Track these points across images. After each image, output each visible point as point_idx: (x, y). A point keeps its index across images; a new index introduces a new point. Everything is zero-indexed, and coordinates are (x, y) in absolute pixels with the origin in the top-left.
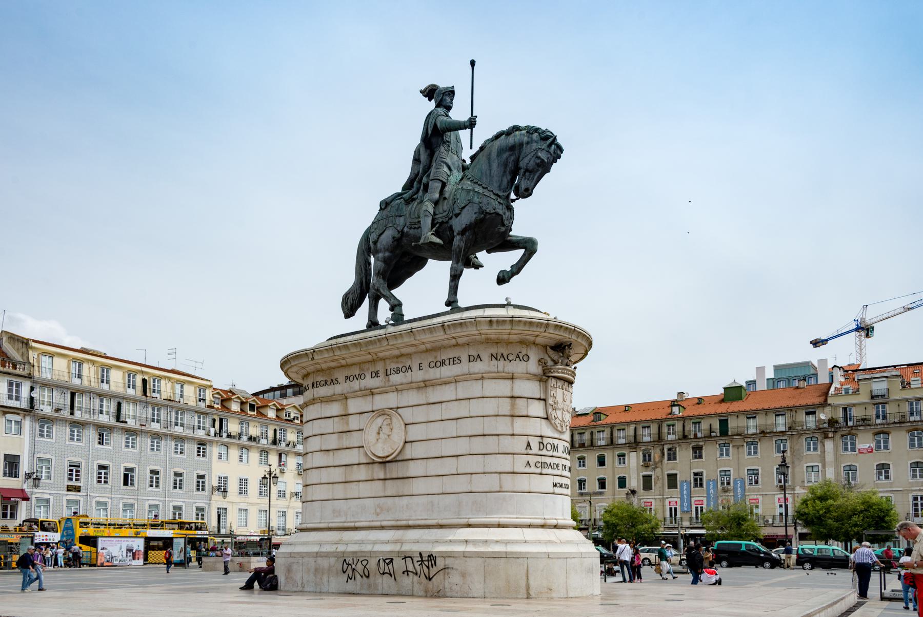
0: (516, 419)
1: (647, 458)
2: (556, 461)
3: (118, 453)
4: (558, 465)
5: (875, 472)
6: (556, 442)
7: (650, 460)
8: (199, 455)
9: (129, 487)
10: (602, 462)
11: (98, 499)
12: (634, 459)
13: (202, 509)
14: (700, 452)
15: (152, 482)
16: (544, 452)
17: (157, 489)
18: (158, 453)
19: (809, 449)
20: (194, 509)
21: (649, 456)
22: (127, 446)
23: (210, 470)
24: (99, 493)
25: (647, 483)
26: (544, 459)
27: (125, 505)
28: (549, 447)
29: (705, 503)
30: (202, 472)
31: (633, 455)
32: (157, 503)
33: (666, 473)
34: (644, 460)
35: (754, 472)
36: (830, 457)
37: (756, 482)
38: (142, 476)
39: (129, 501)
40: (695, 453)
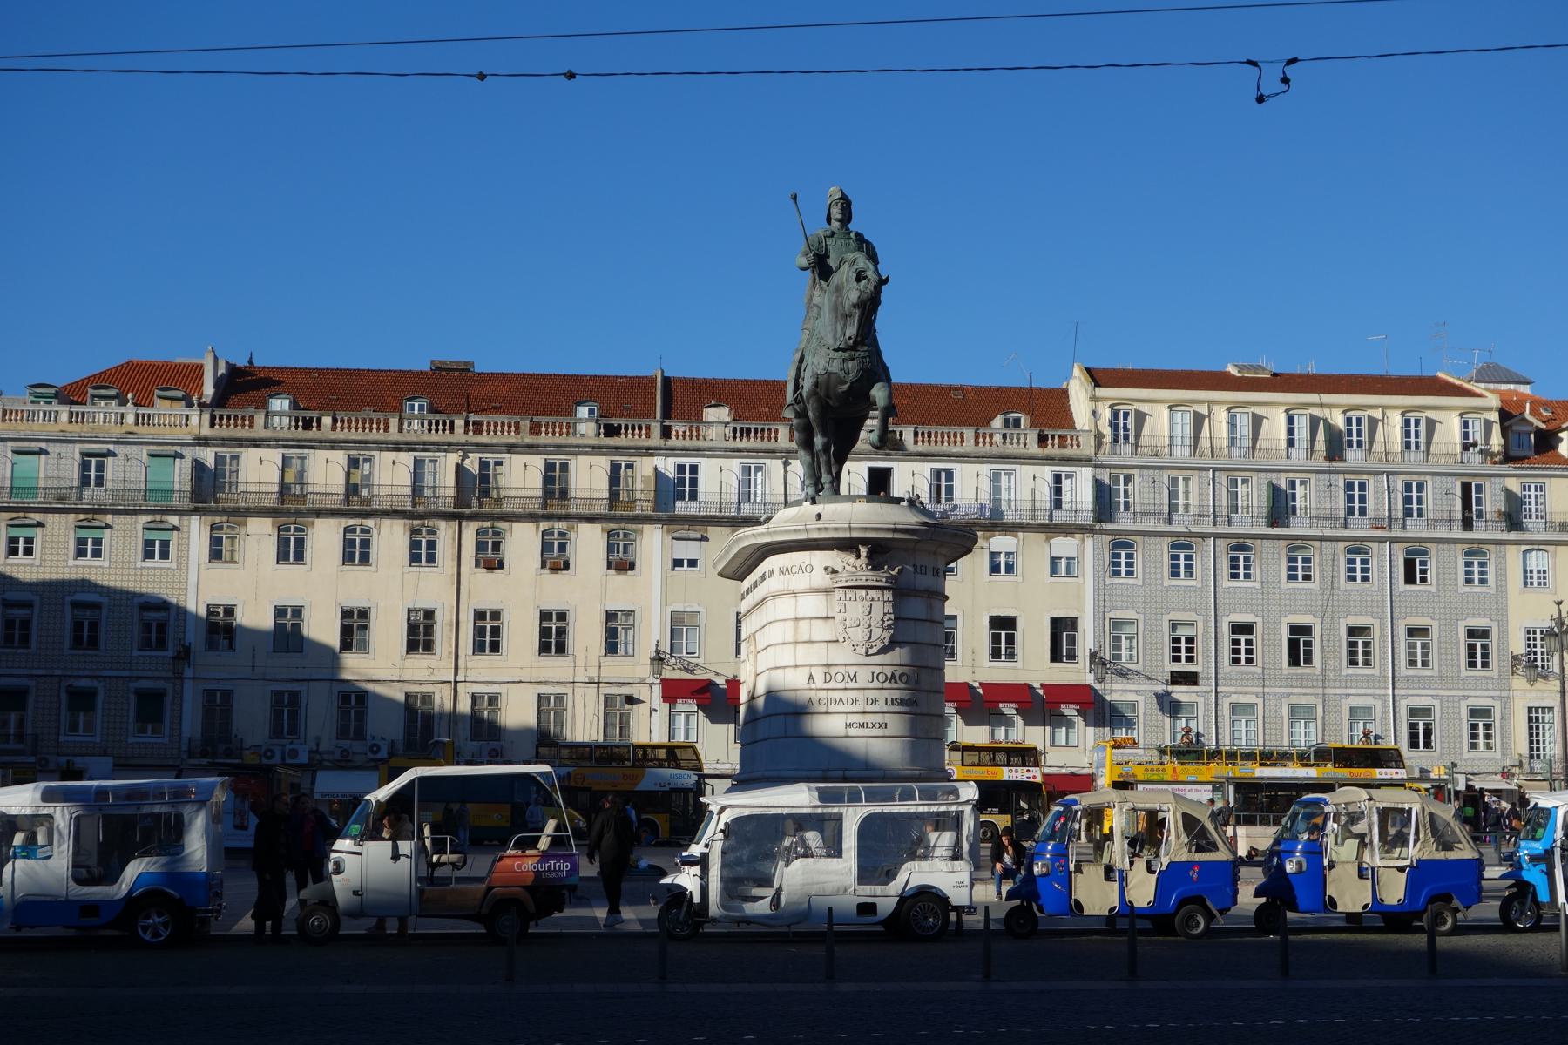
0: (799, 647)
2: (852, 694)
3: (1272, 598)
4: (855, 701)
6: (852, 671)
8: (1469, 582)
9: (1302, 670)
11: (1234, 698)
13: (1485, 713)
15: (1353, 653)
16: (832, 685)
17: (1367, 671)
18: (1366, 585)
20: (1464, 713)
22: (1293, 578)
23: (1502, 616)
24: (1240, 687)
26: (831, 694)
27: (1293, 710)
28: (839, 677)
30: (1479, 623)
32: (1369, 701)
38: (1330, 642)
39: (1304, 700)
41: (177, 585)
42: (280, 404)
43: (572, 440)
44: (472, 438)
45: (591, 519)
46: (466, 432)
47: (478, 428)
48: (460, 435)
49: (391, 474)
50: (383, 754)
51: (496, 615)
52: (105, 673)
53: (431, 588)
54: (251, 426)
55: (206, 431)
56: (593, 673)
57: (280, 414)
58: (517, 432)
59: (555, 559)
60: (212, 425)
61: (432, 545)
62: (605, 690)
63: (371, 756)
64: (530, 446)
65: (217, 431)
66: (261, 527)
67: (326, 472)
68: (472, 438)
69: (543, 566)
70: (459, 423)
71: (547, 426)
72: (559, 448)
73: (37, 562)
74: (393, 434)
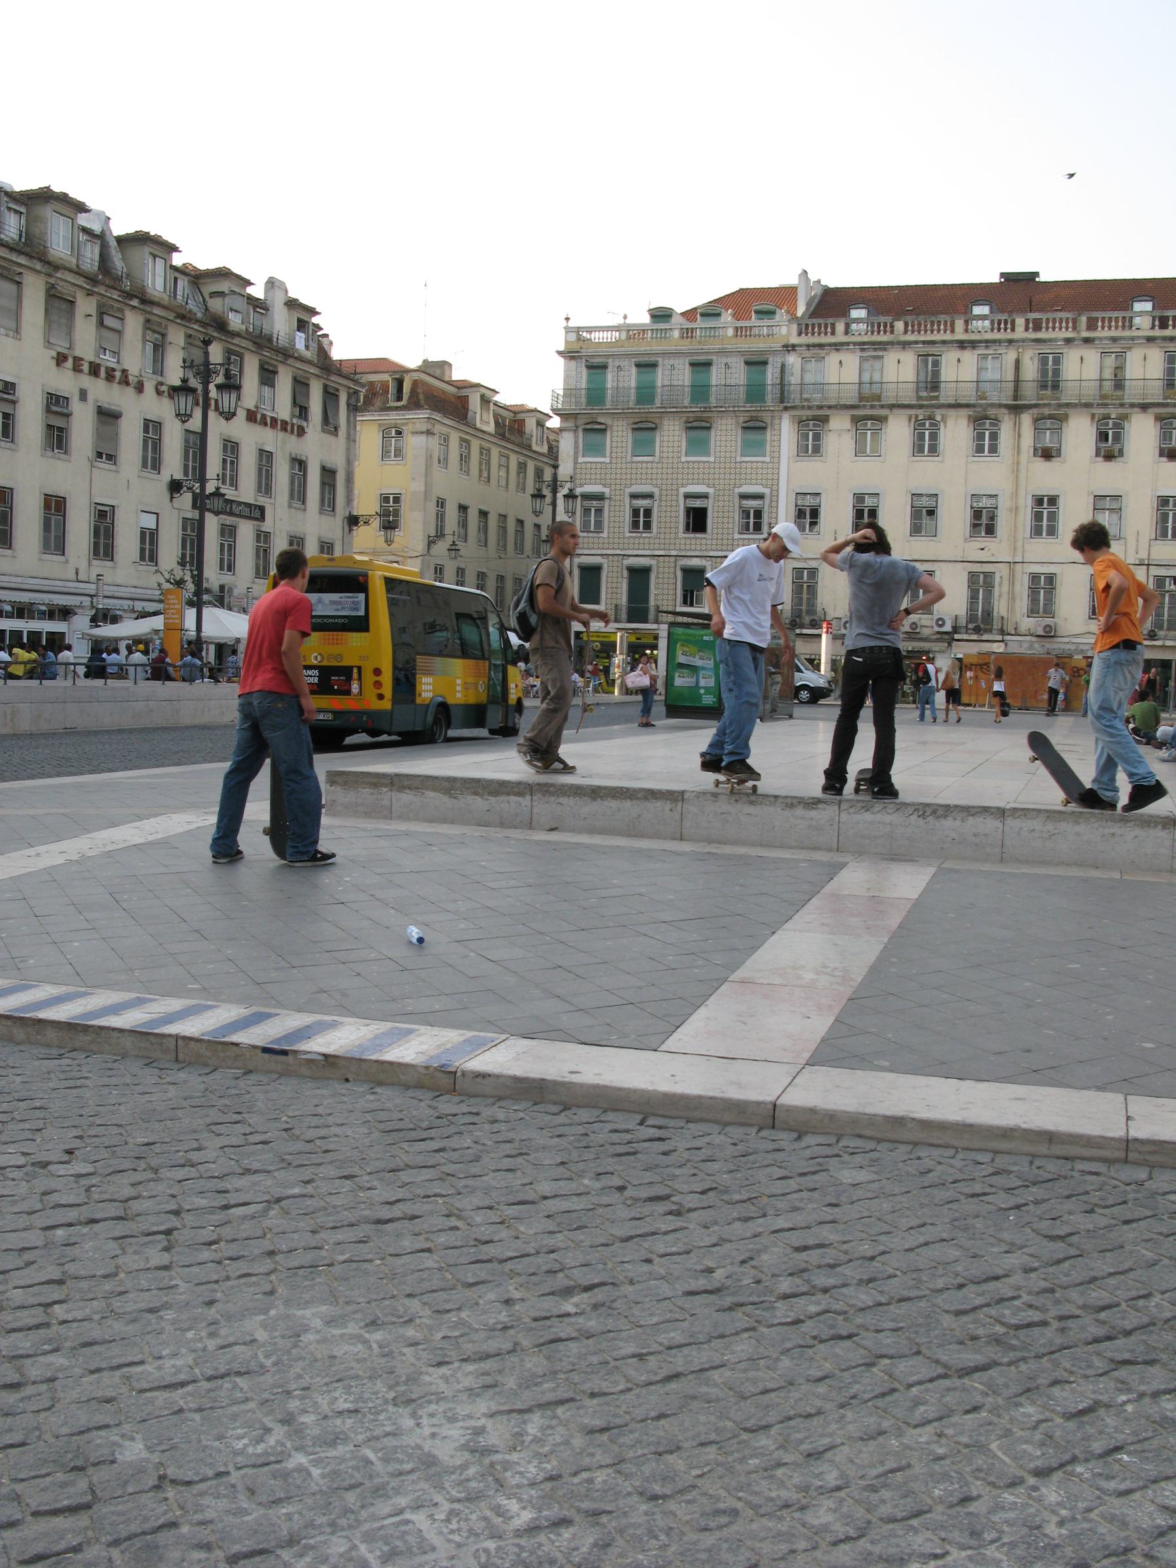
41: (770, 476)
42: (856, 313)
43: (1127, 333)
44: (1032, 335)
45: (1144, 407)
46: (1027, 329)
47: (1037, 327)
48: (1020, 333)
49: (959, 371)
50: (948, 628)
51: (1053, 500)
52: (712, 554)
53: (992, 476)
54: (833, 333)
55: (794, 340)
56: (1143, 555)
57: (858, 321)
58: (1074, 328)
59: (1109, 447)
60: (800, 334)
61: (994, 437)
62: (1155, 571)
63: (937, 629)
64: (1087, 341)
65: (804, 339)
66: (840, 423)
67: (899, 370)
68: (1032, 335)
69: (1097, 455)
70: (1020, 322)
71: (1103, 319)
72: (1114, 340)
73: (657, 459)
74: (960, 335)
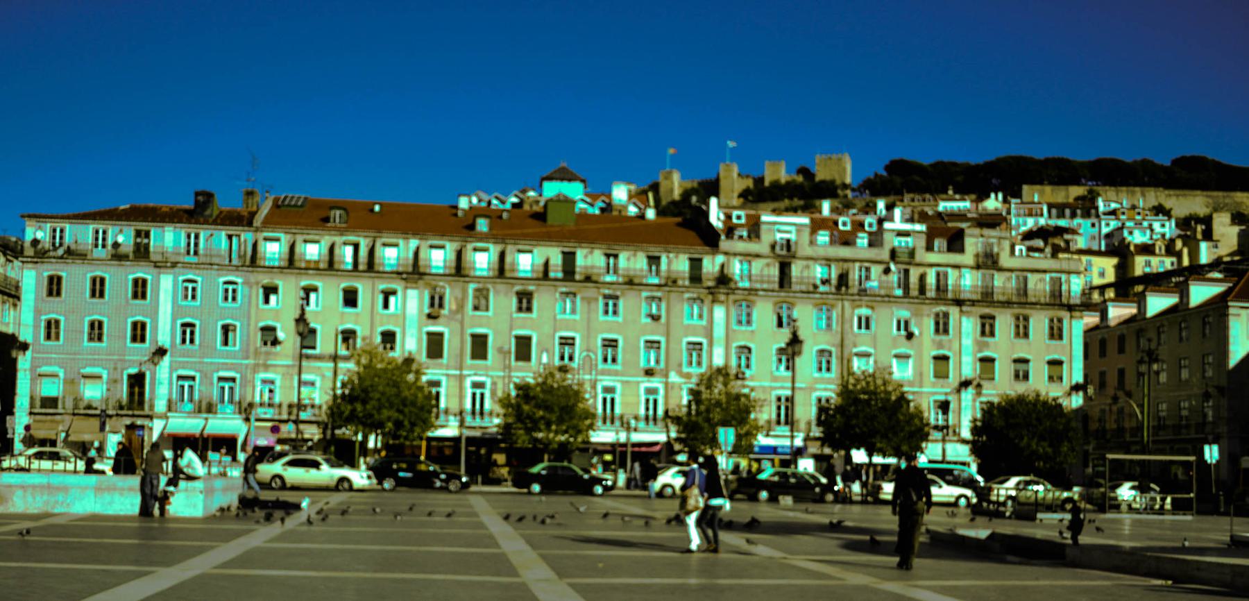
1: (437, 302)
5: (775, 359)
7: (441, 306)
10: (350, 299)
12: (412, 301)
14: (529, 302)
19: (606, 312)
21: (441, 298)
25: (435, 345)
29: (662, 392)
31: (413, 294)
33: (559, 334)
34: (432, 305)
35: (611, 344)
36: (719, 331)
37: (614, 360)
40: (520, 301)
